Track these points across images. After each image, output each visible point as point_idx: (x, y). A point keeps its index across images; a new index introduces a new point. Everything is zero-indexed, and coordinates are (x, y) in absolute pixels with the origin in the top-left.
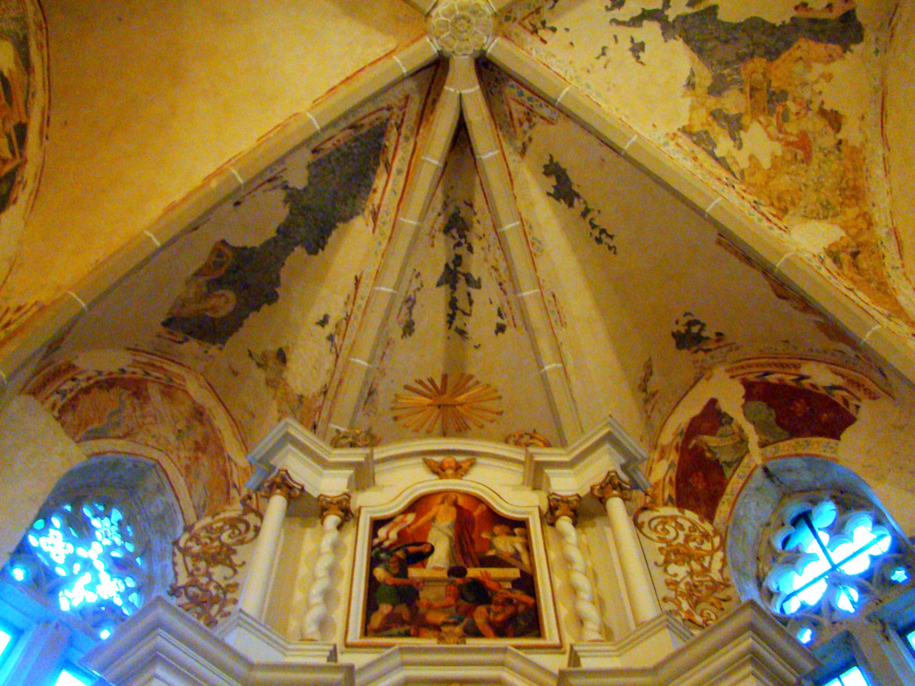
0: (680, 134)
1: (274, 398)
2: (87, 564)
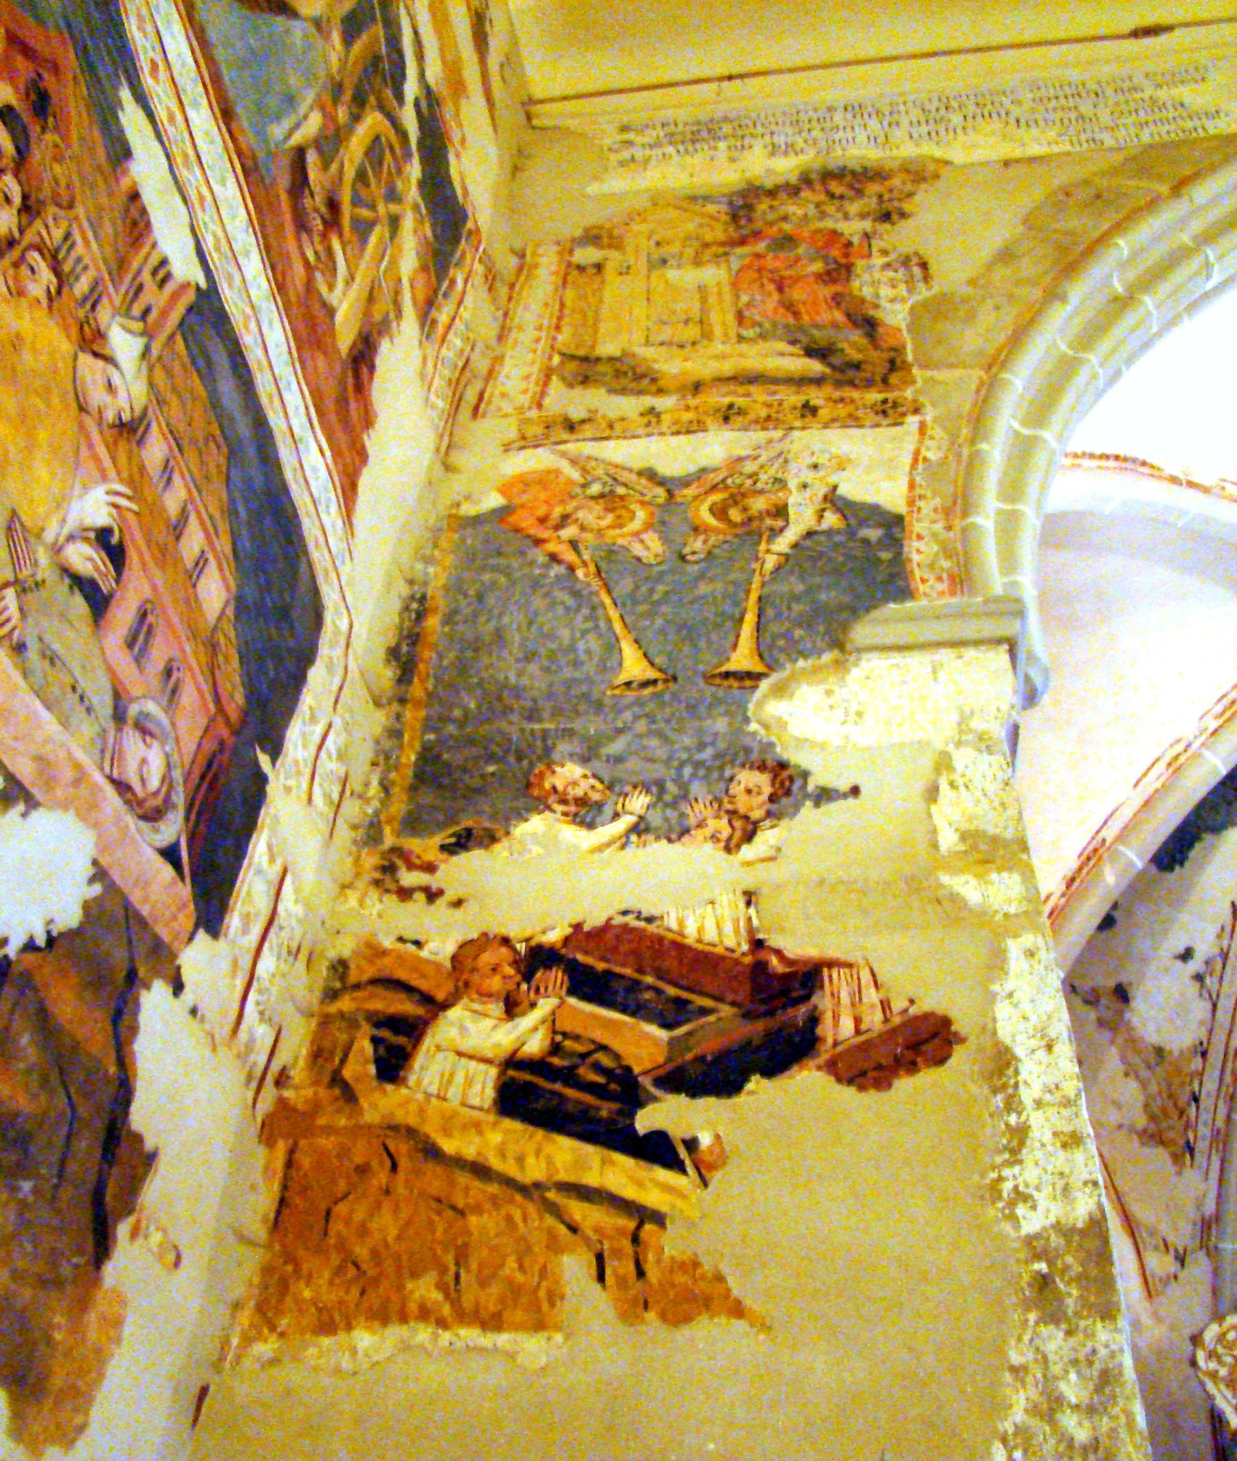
1: (1112, 1042)
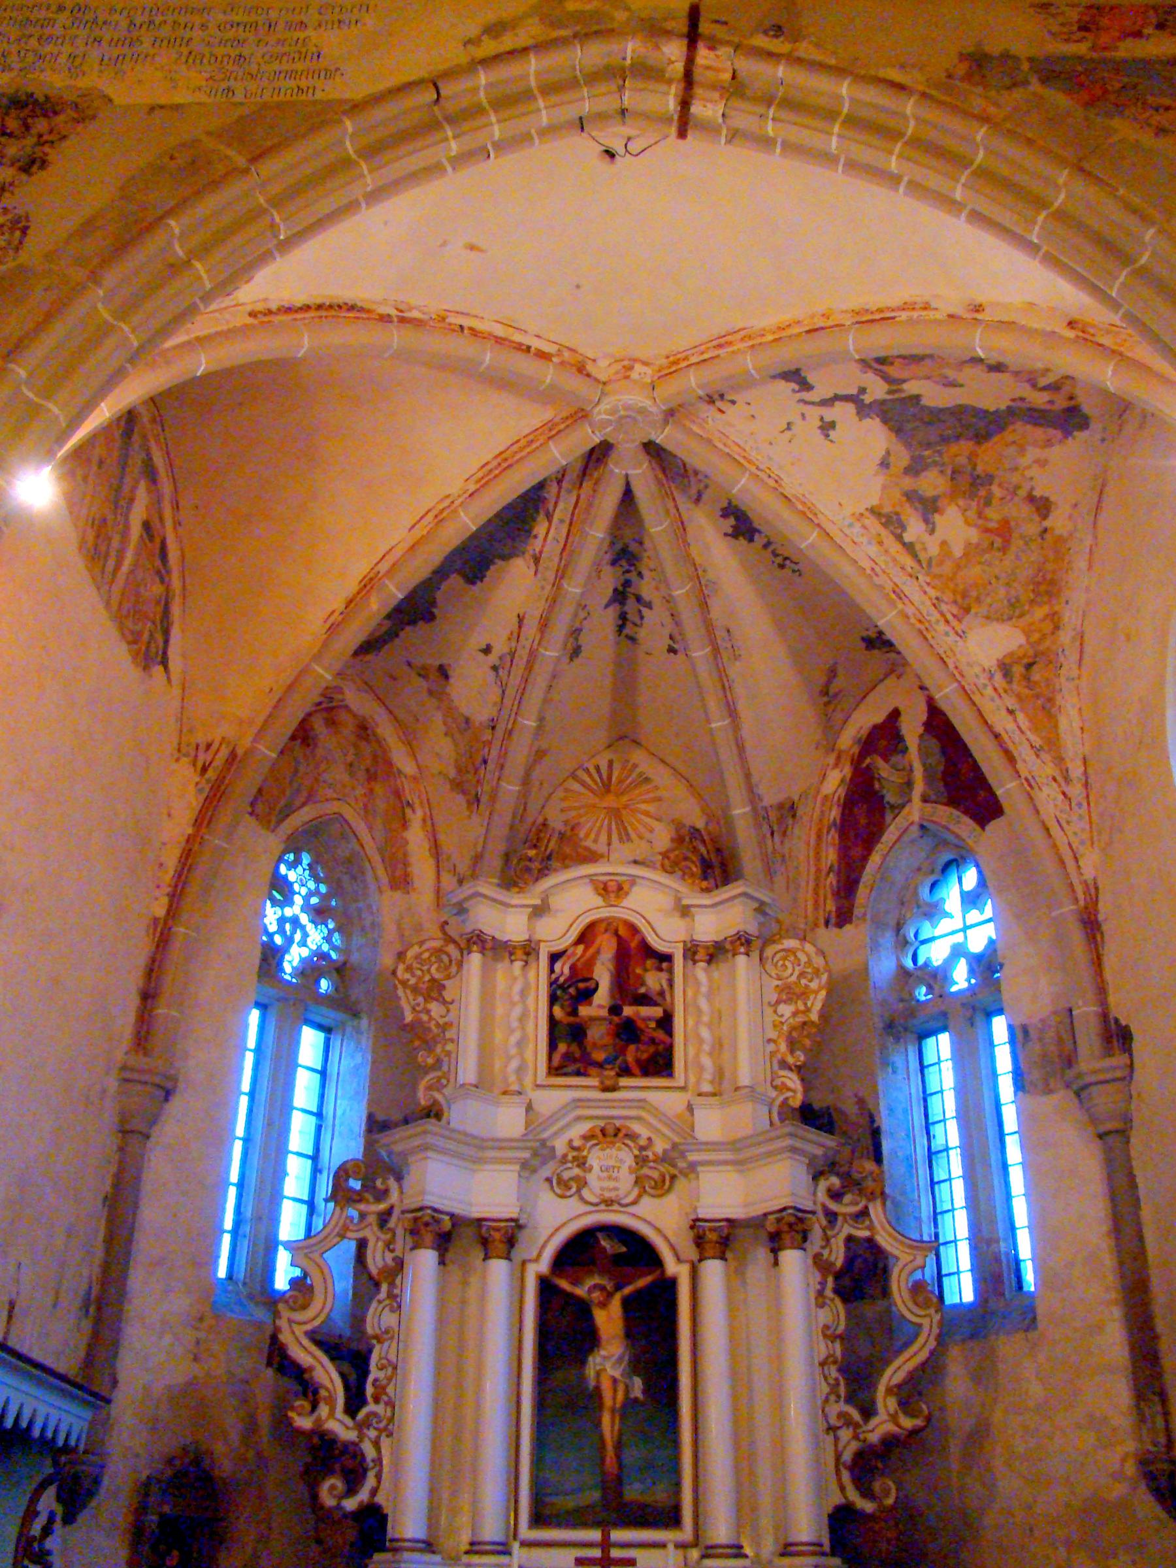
0: (867, 514)
1: (438, 708)
2: (295, 921)
